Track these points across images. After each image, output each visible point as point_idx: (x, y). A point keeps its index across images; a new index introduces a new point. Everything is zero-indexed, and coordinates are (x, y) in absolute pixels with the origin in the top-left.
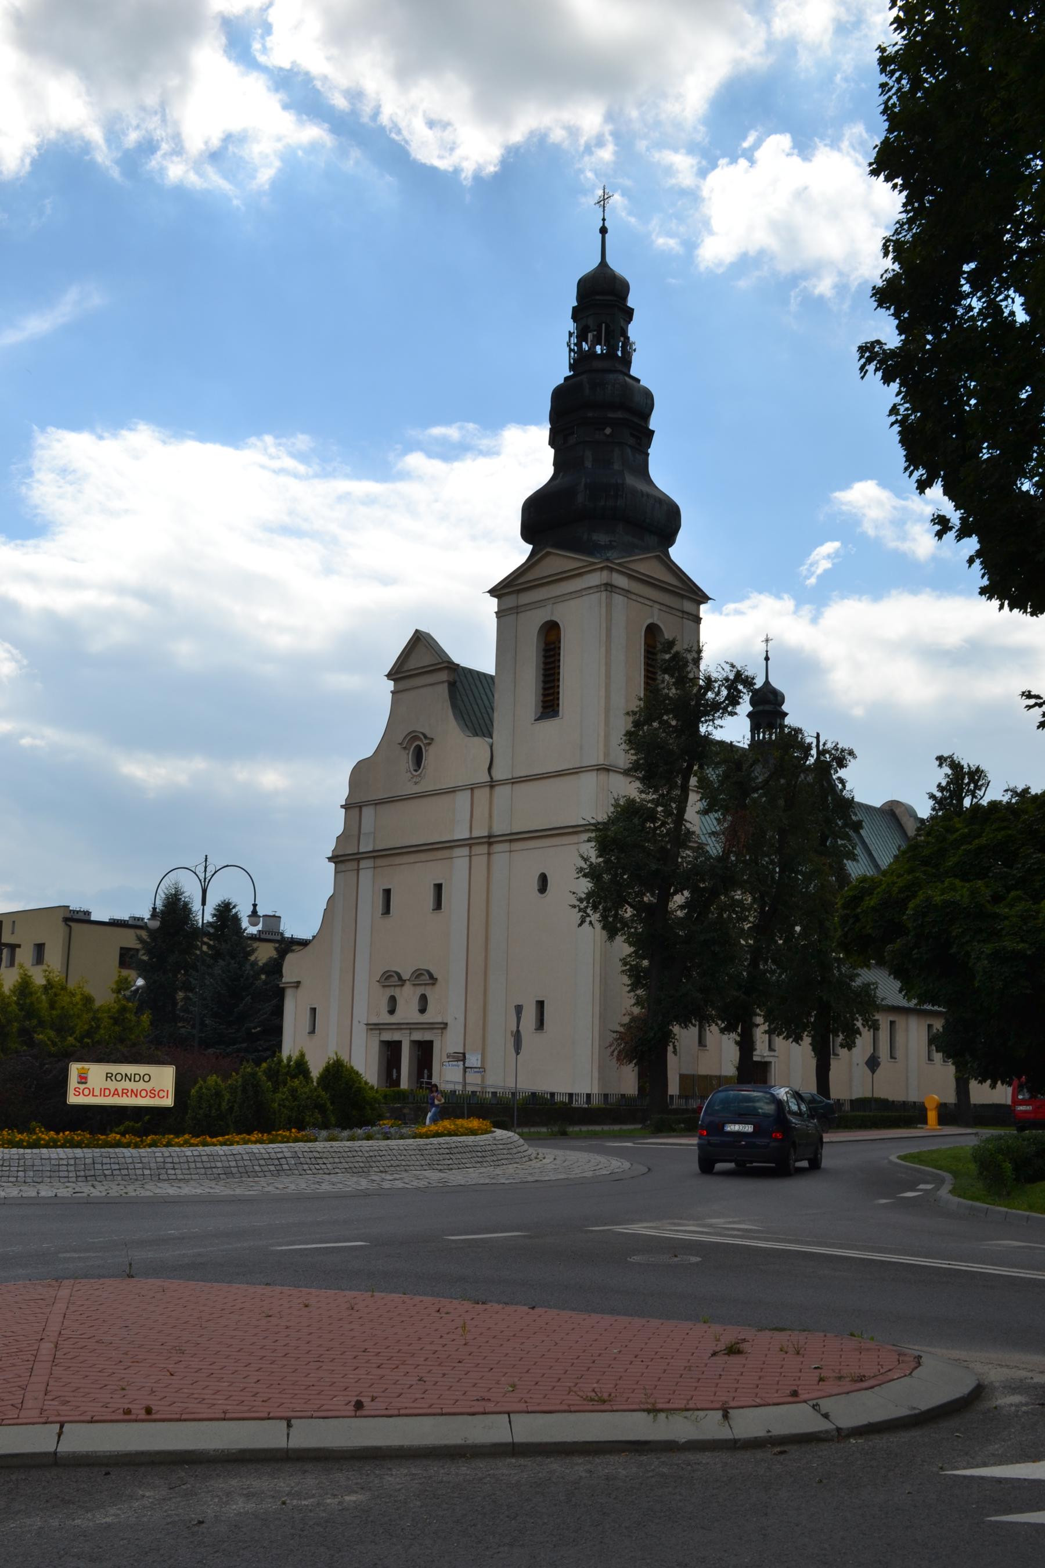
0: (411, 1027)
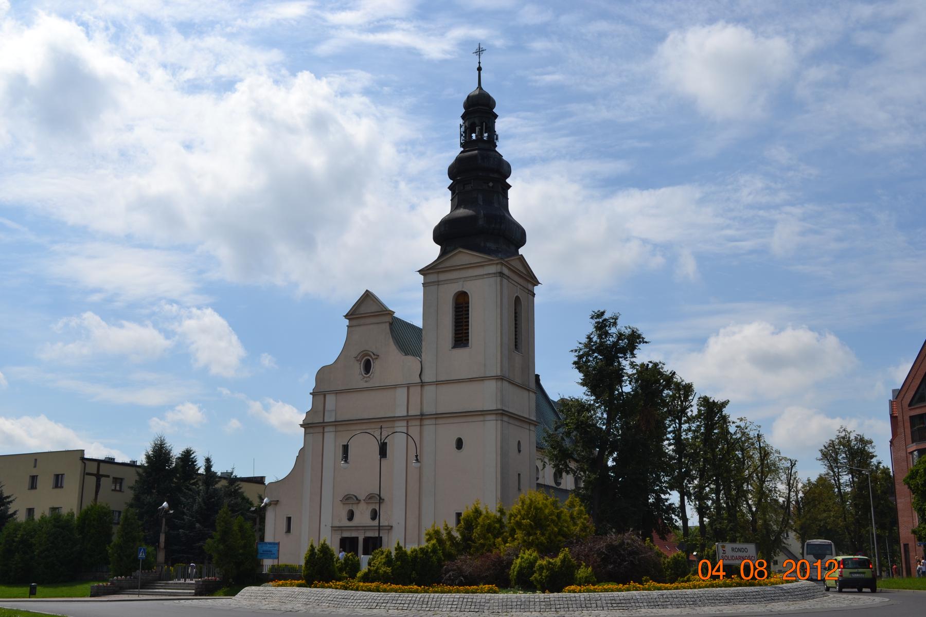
0: (365, 528)
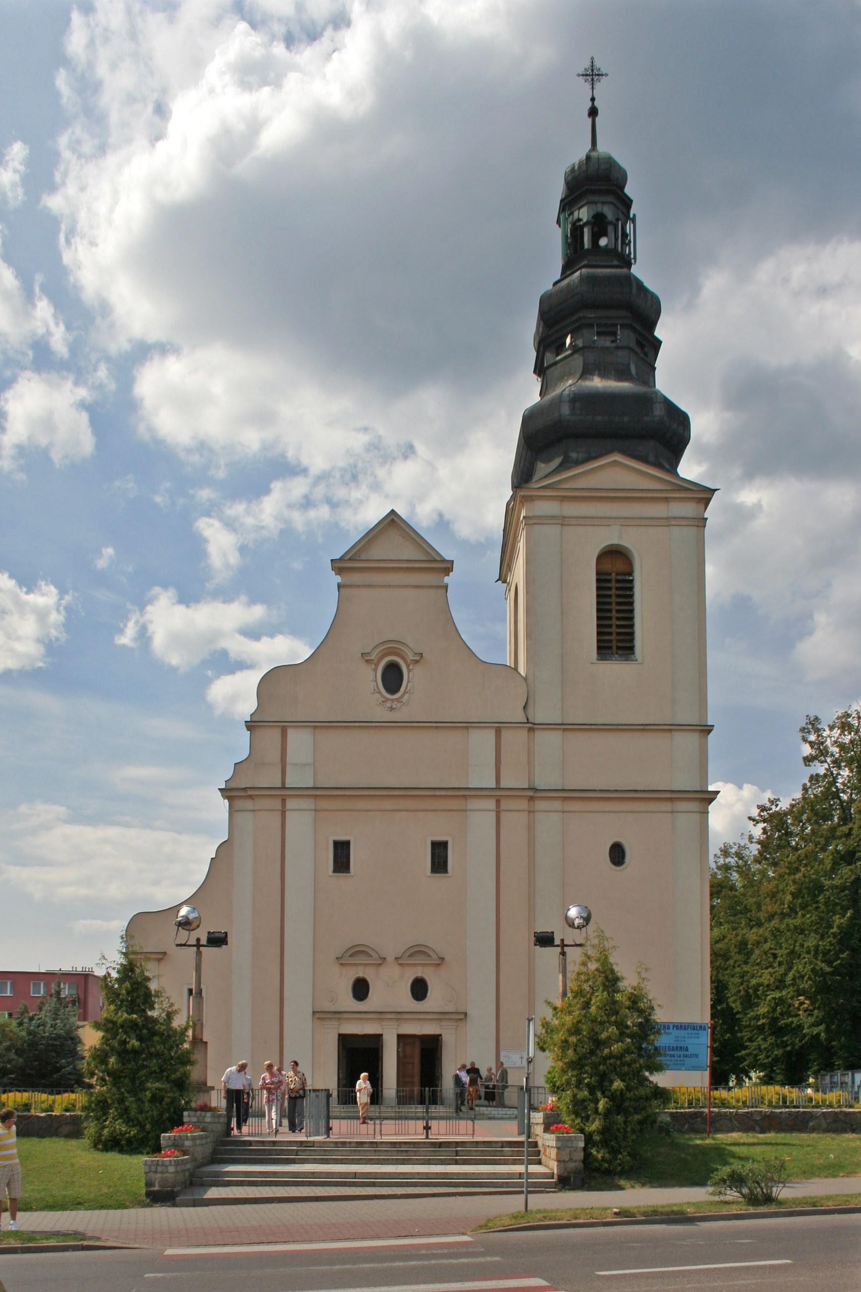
0: (399, 1016)
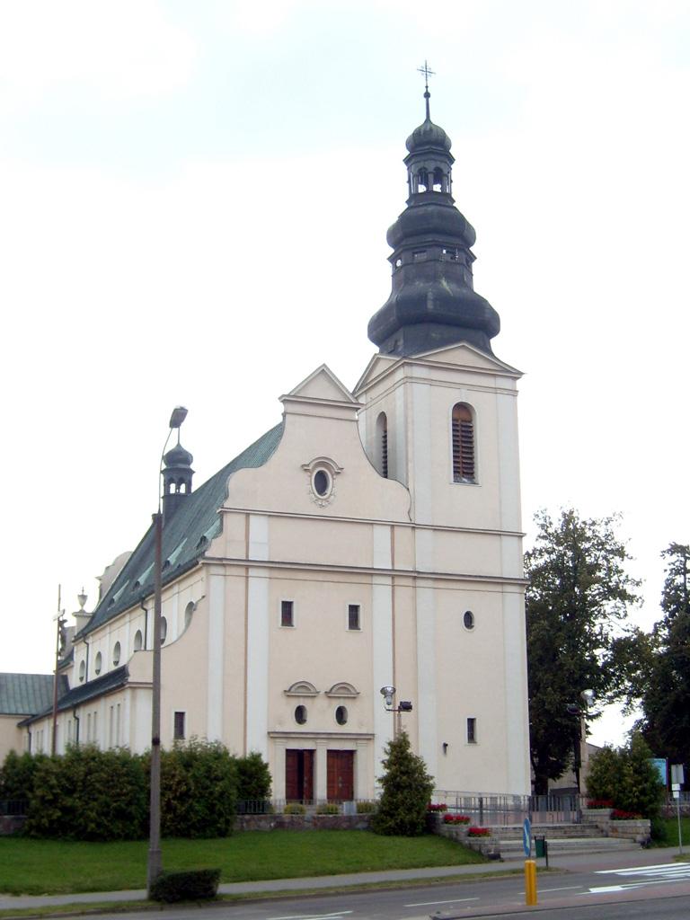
0: (330, 736)
